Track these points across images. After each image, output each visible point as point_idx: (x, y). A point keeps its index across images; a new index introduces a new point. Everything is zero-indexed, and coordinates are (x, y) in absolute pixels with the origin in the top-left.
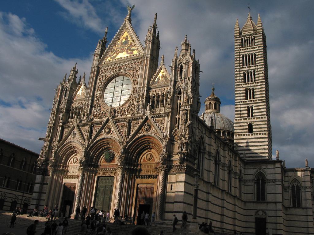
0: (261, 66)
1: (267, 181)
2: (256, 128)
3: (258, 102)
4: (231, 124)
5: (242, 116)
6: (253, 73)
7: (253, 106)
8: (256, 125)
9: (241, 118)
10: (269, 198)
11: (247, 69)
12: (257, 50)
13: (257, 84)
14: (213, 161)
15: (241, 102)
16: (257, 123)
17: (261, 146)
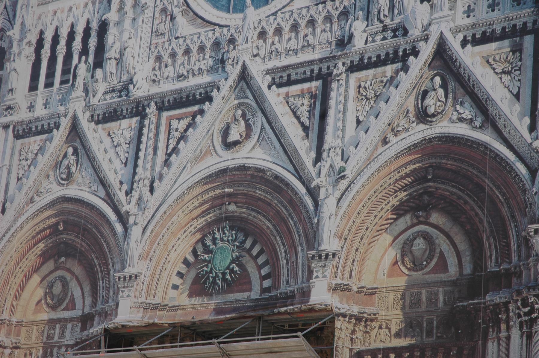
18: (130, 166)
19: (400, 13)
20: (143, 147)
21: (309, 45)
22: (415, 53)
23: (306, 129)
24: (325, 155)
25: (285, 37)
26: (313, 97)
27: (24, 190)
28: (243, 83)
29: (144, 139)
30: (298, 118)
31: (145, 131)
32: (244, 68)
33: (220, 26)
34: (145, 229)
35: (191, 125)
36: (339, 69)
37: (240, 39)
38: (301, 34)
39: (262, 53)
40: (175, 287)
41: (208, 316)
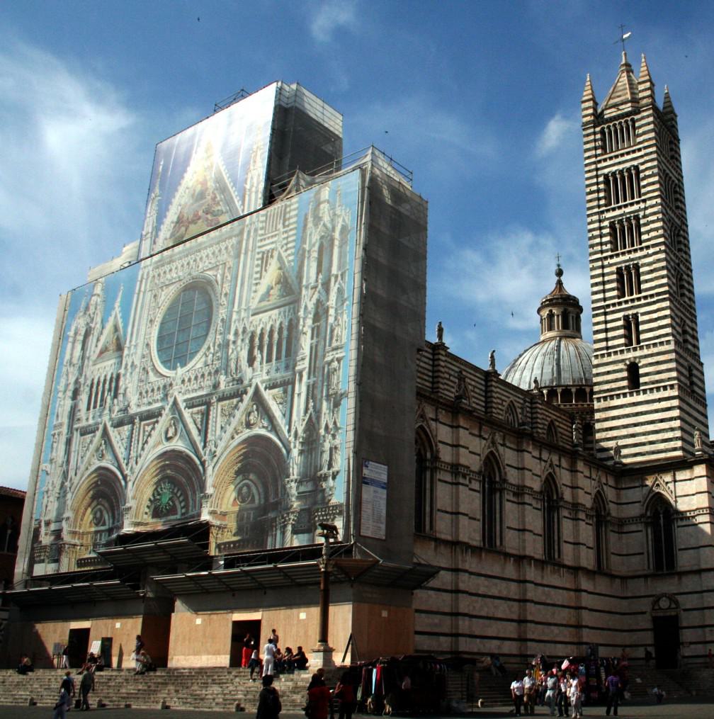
0: (654, 202)
1: (675, 516)
2: (647, 374)
3: (649, 300)
4: (587, 369)
5: (610, 343)
6: (633, 222)
7: (637, 313)
8: (646, 366)
9: (610, 351)
10: (684, 560)
11: (618, 212)
12: (642, 156)
13: (645, 252)
14: (467, 486)
15: (608, 306)
16: (650, 360)
17: (662, 421)
18: (128, 450)
19: (240, 372)
20: (133, 440)
21: (202, 387)
22: (246, 393)
23: (199, 431)
24: (207, 444)
25: (192, 383)
26: (203, 414)
27: (84, 463)
28: (174, 407)
29: (134, 436)
30: (196, 425)
31: (134, 431)
32: (175, 399)
33: (167, 377)
34: (134, 483)
35: (153, 429)
36: (214, 400)
37: (174, 383)
38: (199, 381)
39: (183, 391)
40: (146, 513)
41: (160, 528)
